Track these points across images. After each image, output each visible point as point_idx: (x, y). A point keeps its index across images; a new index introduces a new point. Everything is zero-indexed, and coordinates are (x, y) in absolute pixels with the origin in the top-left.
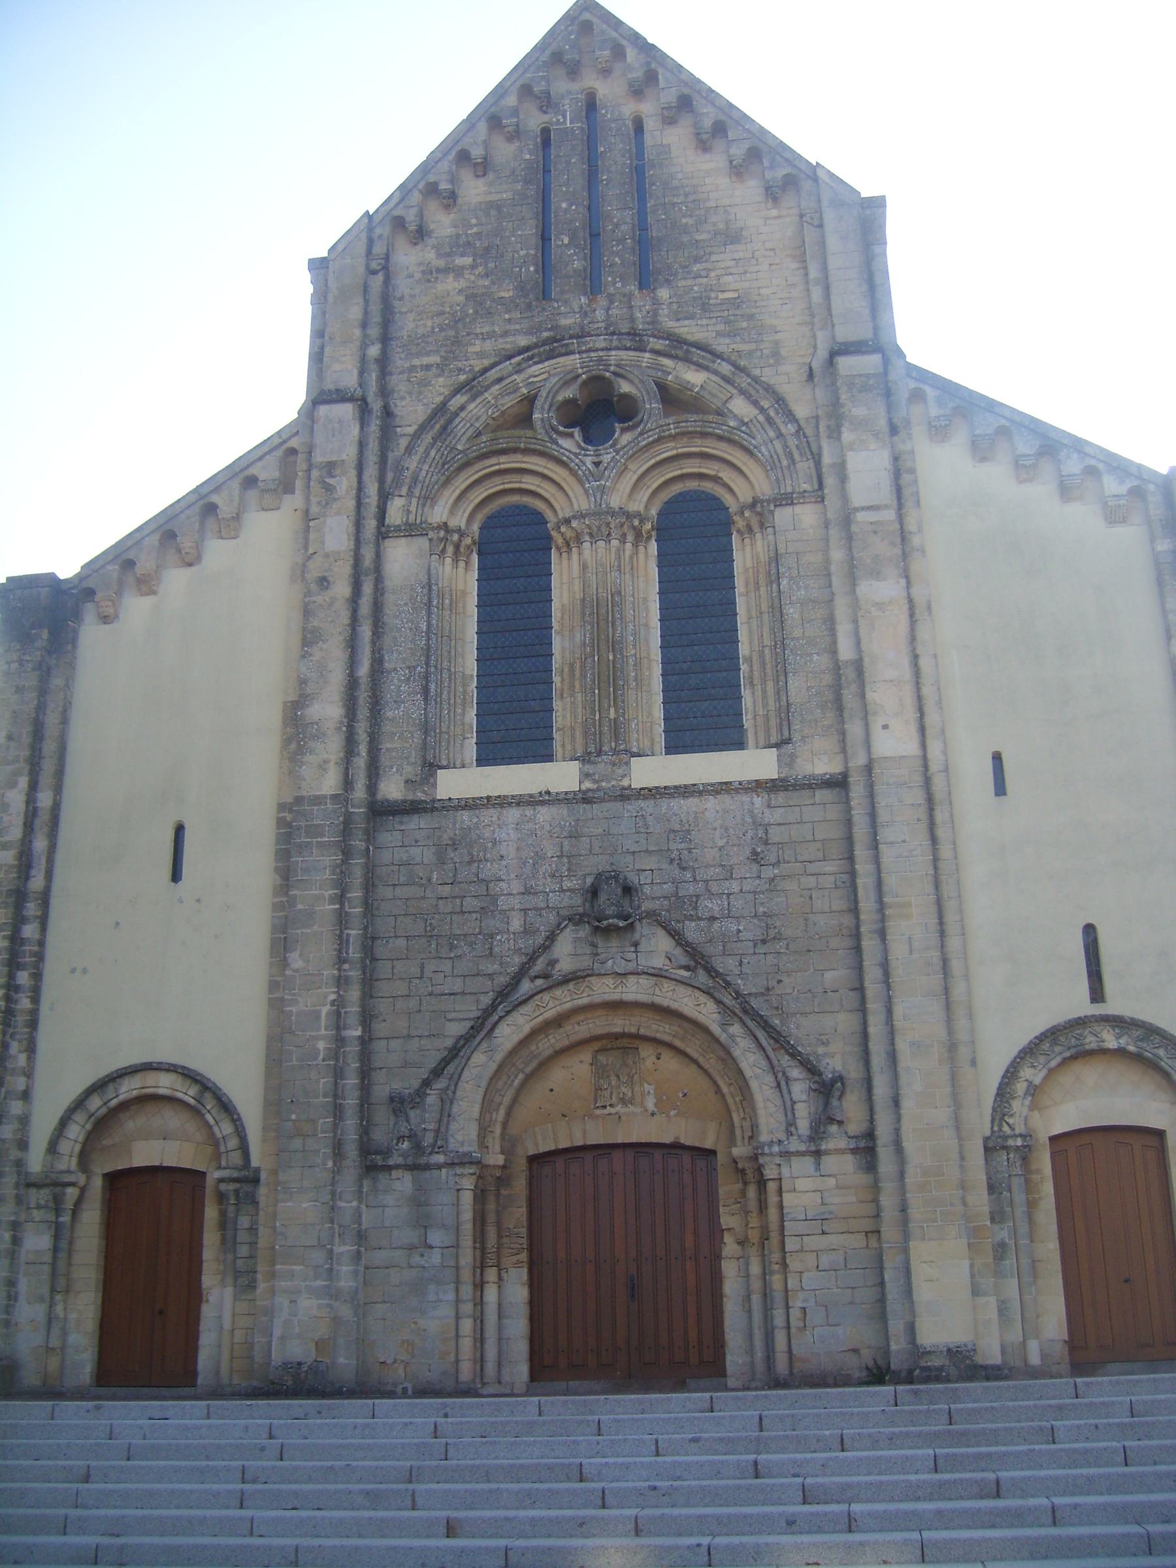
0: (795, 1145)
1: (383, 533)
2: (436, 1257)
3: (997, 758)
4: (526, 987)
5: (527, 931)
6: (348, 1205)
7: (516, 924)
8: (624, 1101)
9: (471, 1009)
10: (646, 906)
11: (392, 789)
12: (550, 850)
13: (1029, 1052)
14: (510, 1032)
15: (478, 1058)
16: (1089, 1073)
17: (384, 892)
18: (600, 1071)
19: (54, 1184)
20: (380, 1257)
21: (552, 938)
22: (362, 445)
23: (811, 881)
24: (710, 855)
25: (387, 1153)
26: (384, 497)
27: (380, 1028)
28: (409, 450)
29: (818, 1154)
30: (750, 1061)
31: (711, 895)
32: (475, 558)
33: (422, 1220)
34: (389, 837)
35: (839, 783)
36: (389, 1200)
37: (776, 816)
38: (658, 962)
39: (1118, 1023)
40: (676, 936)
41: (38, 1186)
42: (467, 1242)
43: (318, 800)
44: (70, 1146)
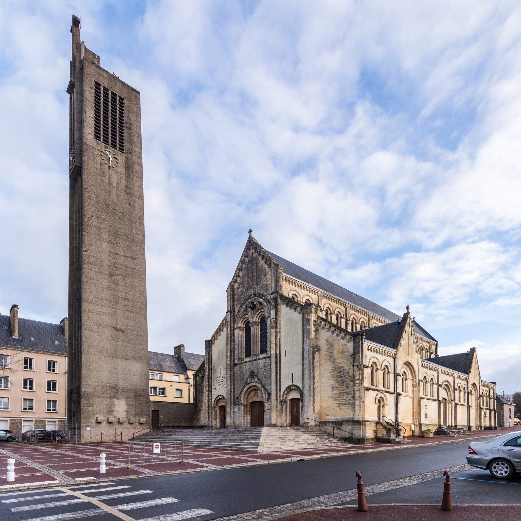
0: (266, 401)
1: (234, 329)
4: (246, 384)
5: (246, 378)
6: (232, 409)
8: (257, 396)
9: (242, 387)
10: (256, 374)
11: (236, 362)
13: (286, 389)
14: (245, 389)
15: (243, 393)
17: (236, 374)
18: (255, 393)
19: (214, 408)
24: (260, 367)
27: (236, 390)
29: (268, 402)
30: (263, 392)
33: (239, 410)
34: (236, 368)
36: (237, 408)
37: (266, 361)
38: (256, 381)
39: (295, 386)
40: (257, 377)
44: (215, 404)
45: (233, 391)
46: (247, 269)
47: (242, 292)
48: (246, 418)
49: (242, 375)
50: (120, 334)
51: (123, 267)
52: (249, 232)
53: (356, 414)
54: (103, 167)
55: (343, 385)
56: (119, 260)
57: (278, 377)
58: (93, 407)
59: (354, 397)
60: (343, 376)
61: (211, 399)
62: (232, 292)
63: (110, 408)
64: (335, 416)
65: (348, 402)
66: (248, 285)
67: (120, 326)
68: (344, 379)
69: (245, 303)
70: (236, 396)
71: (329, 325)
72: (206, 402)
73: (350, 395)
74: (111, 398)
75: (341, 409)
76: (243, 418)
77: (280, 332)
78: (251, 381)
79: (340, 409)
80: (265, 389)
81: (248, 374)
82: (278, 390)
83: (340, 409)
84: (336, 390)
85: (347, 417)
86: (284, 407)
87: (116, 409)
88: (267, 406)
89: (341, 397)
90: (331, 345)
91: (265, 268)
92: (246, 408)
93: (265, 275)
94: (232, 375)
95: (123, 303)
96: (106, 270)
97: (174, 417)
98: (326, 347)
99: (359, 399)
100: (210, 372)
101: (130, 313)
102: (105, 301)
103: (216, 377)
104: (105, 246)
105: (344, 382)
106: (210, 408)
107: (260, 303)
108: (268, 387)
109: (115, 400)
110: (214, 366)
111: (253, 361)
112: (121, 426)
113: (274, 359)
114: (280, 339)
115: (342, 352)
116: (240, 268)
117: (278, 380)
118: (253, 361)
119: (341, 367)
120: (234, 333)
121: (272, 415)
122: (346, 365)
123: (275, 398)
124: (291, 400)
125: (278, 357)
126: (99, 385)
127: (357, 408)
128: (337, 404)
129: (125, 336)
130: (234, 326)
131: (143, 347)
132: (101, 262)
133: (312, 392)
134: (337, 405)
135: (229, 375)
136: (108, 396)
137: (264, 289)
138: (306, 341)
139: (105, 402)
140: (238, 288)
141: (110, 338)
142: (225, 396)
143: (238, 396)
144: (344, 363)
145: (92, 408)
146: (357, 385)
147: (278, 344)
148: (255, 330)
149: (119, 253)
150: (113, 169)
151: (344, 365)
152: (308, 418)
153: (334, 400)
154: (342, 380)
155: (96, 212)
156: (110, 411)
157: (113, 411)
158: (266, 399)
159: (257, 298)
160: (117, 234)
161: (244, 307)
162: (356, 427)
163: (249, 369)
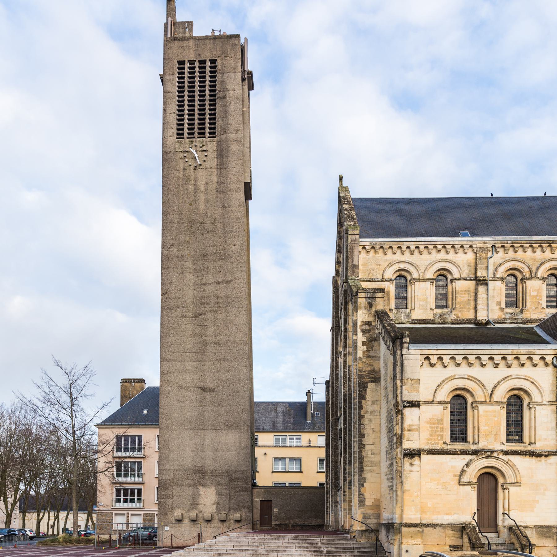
50: (208, 395)
51: (212, 300)
54: (187, 171)
56: (208, 292)
58: (172, 499)
63: (193, 499)
67: (209, 384)
74: (195, 485)
87: (202, 501)
95: (213, 351)
96: (189, 310)
97: (296, 510)
101: (222, 362)
102: (189, 354)
104: (190, 278)
109: (201, 488)
112: (209, 525)
126: (180, 470)
129: (215, 397)
131: (242, 407)
132: (184, 302)
136: (192, 483)
139: (189, 491)
141: (195, 403)
145: (171, 500)
149: (208, 281)
150: (201, 167)
155: (177, 237)
156: (194, 504)
157: (198, 504)
160: (205, 256)
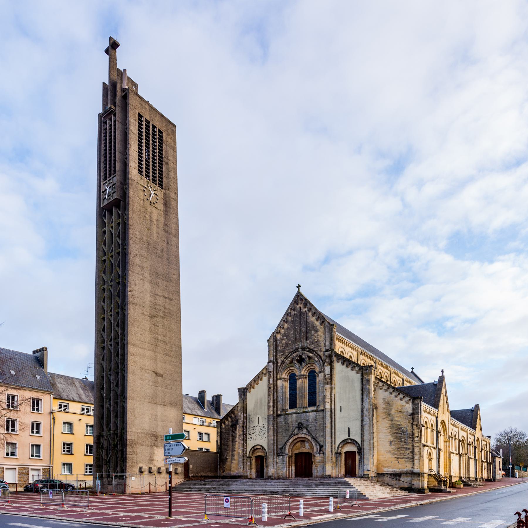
1: (277, 379)
2: (284, 465)
3: (341, 407)
4: (292, 435)
5: (292, 429)
6: (275, 459)
7: (291, 428)
8: (304, 447)
9: (287, 438)
10: (304, 426)
11: (279, 412)
12: (295, 420)
13: (341, 443)
14: (291, 440)
15: (288, 443)
16: (349, 445)
17: (279, 425)
18: (301, 444)
19: (250, 457)
20: (279, 465)
21: (295, 430)
22: (274, 368)
23: (320, 423)
24: (310, 420)
25: (279, 454)
26: (277, 374)
27: (279, 440)
28: (280, 368)
29: (320, 454)
30: (314, 444)
31: (310, 424)
32: (288, 381)
33: (283, 461)
34: (279, 418)
35: (323, 410)
36: (280, 459)
37: (317, 415)
38: (305, 432)
40: (307, 429)
41: (248, 458)
42: (287, 463)
43: (271, 415)
44: (251, 454)
45: (276, 442)
46: (293, 322)
47: (287, 344)
48: (290, 468)
49: (287, 426)
50: (159, 379)
51: (162, 308)
52: (297, 287)
53: (415, 467)
55: (401, 441)
56: (159, 301)
57: (333, 430)
58: (136, 455)
59: (413, 453)
60: (401, 433)
61: (246, 448)
62: (274, 343)
63: (150, 456)
64: (392, 468)
65: (407, 456)
66: (295, 338)
67: (159, 371)
68: (402, 435)
69: (291, 355)
70: (279, 447)
71: (387, 387)
72: (240, 451)
73: (409, 450)
74: (151, 446)
75: (400, 463)
76: (287, 468)
77: (334, 388)
78: (298, 433)
79: (399, 462)
80: (316, 441)
81: (295, 425)
82: (333, 443)
83: (399, 462)
84: (394, 445)
85: (405, 470)
86: (339, 459)
87: (156, 458)
88: (318, 457)
89: (399, 451)
90: (388, 405)
91: (316, 325)
92: (290, 459)
93: (317, 331)
94: (275, 426)
95: (162, 346)
96: (147, 311)
98: (384, 406)
99: (418, 454)
100: (245, 420)
101: (167, 357)
102: (147, 344)
103: (252, 426)
105: (402, 438)
106: (245, 458)
107: (310, 358)
108: (319, 439)
109: (155, 448)
110: (249, 415)
111: (302, 413)
112: (160, 475)
113: (329, 413)
114: (334, 395)
115: (401, 411)
116: (285, 320)
117: (333, 433)
118: (302, 413)
119: (399, 425)
120: (277, 383)
121: (327, 467)
122: (405, 424)
123: (330, 450)
124: (346, 453)
125: (332, 412)
126: (142, 433)
127: (416, 462)
128: (395, 457)
129: (163, 381)
130: (277, 377)
131: (179, 392)
132: (144, 303)
133: (372, 446)
134: (395, 459)
135: (272, 426)
136: (150, 444)
137: (315, 345)
138: (366, 400)
139: (147, 450)
140: (282, 340)
141: (151, 383)
142: (266, 447)
143: (282, 446)
144: (402, 421)
145: (136, 456)
146: (416, 442)
147: (333, 399)
148: (303, 383)
149: (159, 294)
151: (402, 423)
152: (368, 470)
153: (392, 454)
154: (400, 437)
156: (151, 460)
157: (153, 460)
158: (317, 450)
159: (306, 352)
160: (157, 273)
161: (289, 359)
162: (415, 478)
163: (297, 420)
